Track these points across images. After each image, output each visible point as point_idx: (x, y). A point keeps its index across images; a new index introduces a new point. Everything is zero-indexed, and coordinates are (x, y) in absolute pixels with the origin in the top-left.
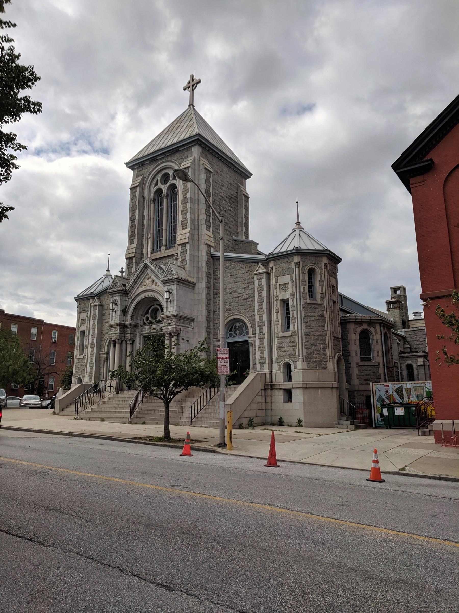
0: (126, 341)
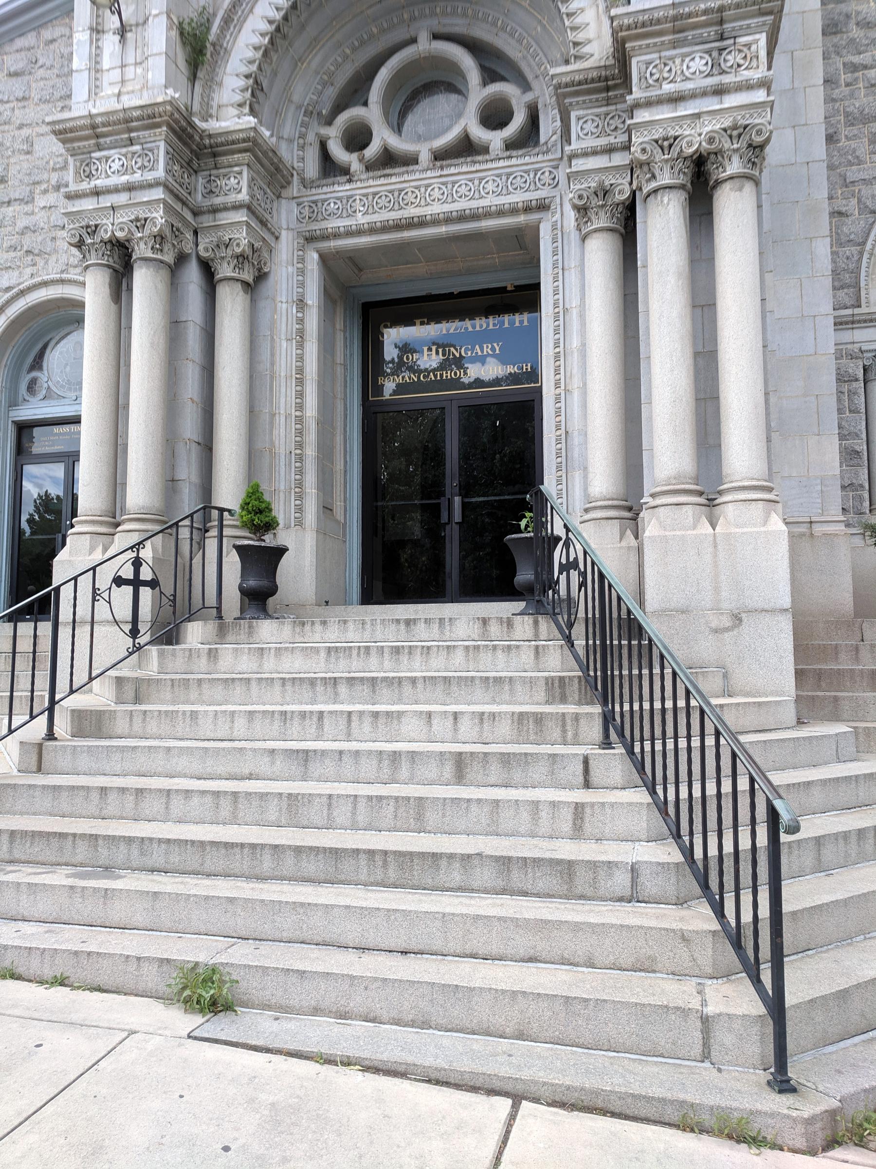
0: (207, 269)
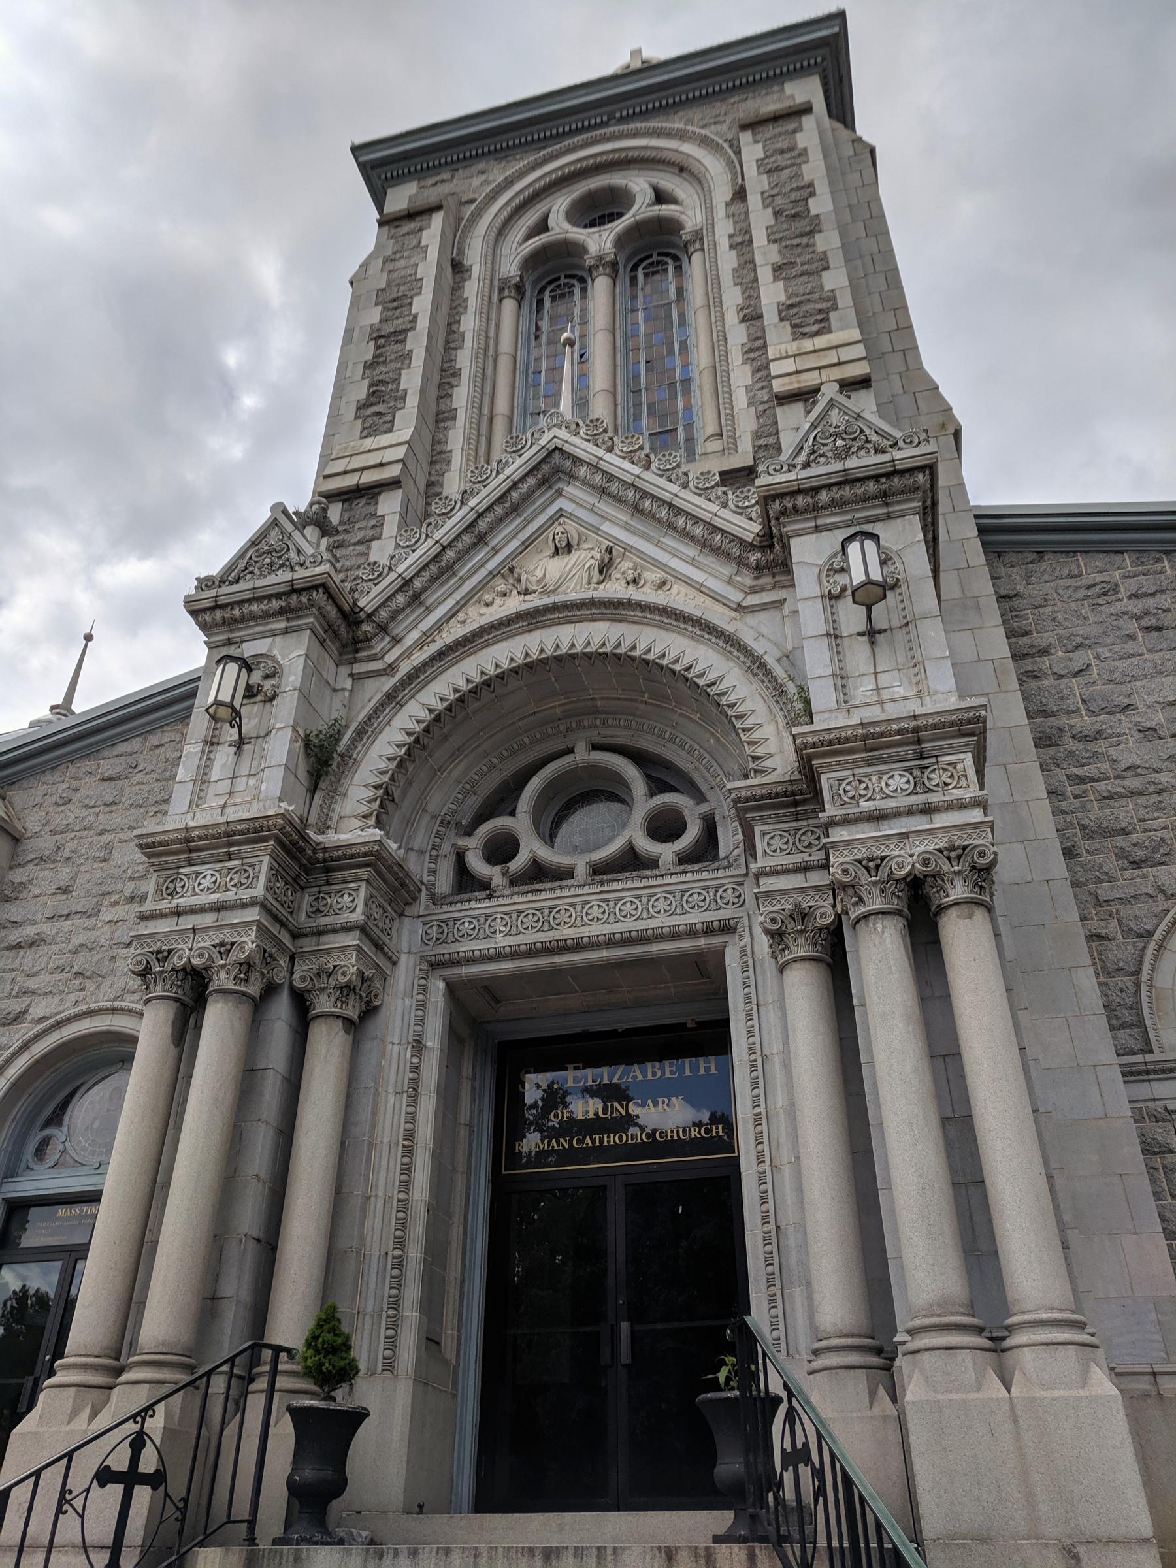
0: (301, 1003)
